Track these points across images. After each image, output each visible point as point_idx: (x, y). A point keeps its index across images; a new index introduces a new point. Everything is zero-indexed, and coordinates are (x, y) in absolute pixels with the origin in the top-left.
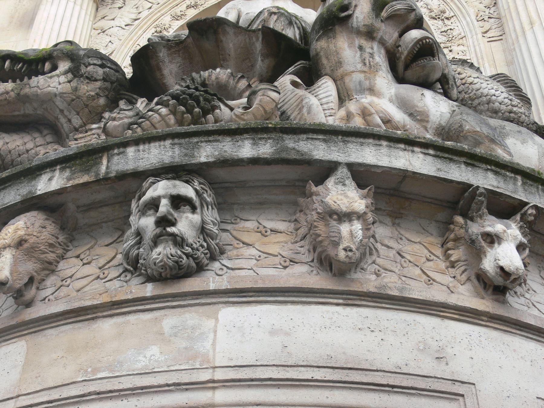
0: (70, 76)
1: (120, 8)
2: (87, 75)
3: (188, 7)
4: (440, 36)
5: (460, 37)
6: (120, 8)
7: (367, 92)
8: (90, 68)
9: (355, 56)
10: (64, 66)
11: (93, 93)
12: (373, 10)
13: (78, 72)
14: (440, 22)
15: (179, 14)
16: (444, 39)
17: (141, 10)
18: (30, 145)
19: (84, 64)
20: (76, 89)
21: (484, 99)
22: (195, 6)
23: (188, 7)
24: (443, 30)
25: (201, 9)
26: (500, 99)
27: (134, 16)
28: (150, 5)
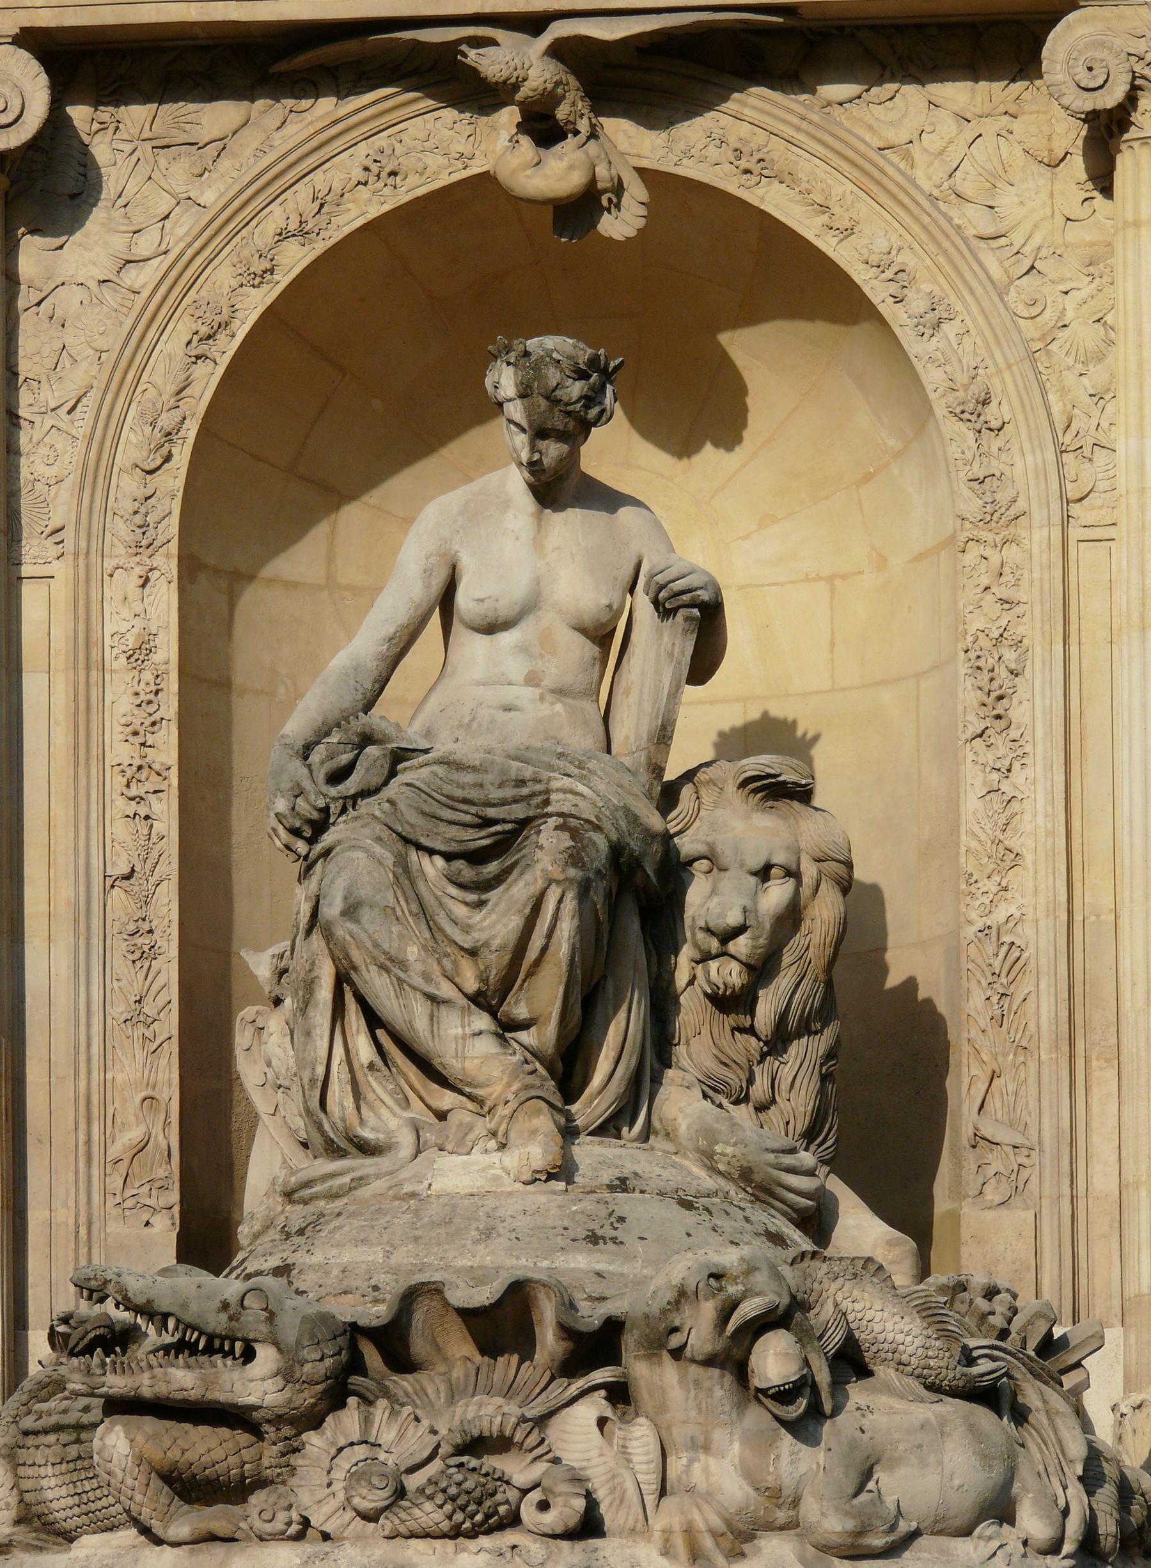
0: (280, 1381)
1: (73, 196)
2: (304, 1378)
3: (283, 236)
4: (966, 492)
5: (1012, 512)
6: (73, 196)
7: (701, 1451)
8: (307, 1368)
9: (687, 1398)
10: (266, 1357)
11: (312, 1400)
12: (716, 1326)
13: (292, 1377)
14: (971, 436)
15: (259, 266)
16: (972, 506)
17: (138, 221)
18: (218, 1454)
19: (299, 1362)
20: (290, 1401)
21: (886, 1346)
22: (302, 233)
23: (283, 236)
24: (978, 471)
25: (320, 247)
26: (910, 1350)
27: (119, 243)
28: (165, 204)
